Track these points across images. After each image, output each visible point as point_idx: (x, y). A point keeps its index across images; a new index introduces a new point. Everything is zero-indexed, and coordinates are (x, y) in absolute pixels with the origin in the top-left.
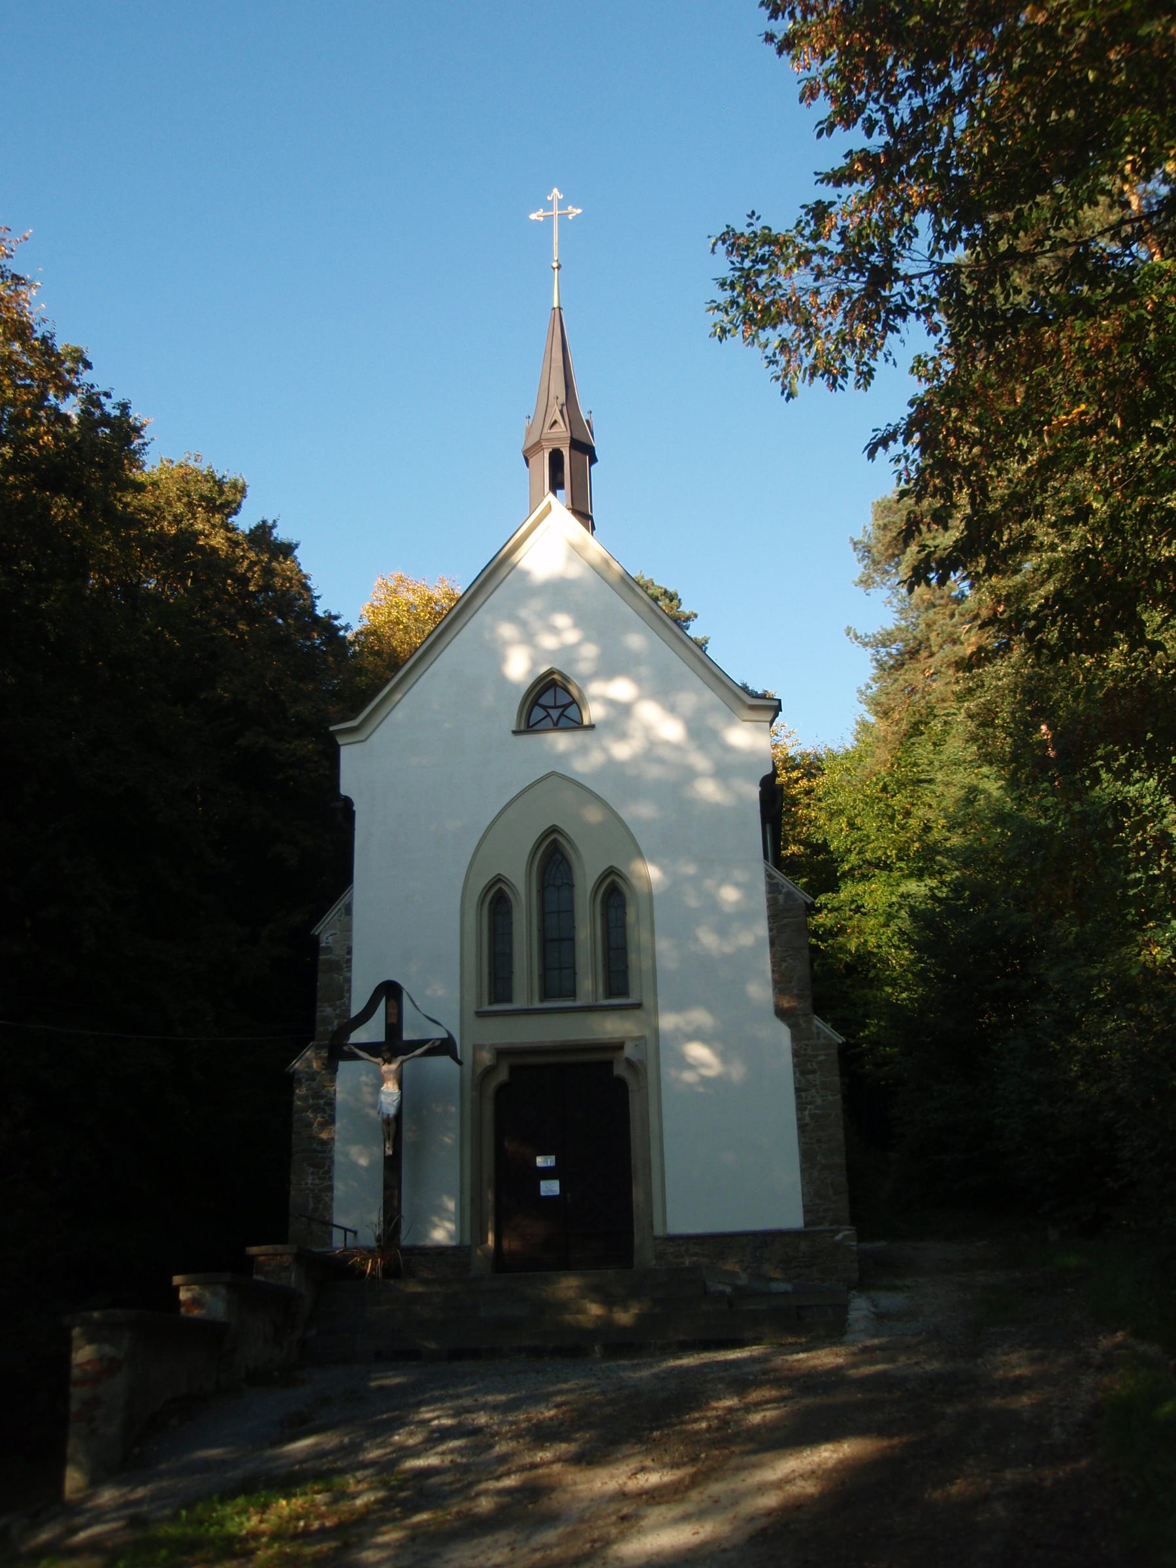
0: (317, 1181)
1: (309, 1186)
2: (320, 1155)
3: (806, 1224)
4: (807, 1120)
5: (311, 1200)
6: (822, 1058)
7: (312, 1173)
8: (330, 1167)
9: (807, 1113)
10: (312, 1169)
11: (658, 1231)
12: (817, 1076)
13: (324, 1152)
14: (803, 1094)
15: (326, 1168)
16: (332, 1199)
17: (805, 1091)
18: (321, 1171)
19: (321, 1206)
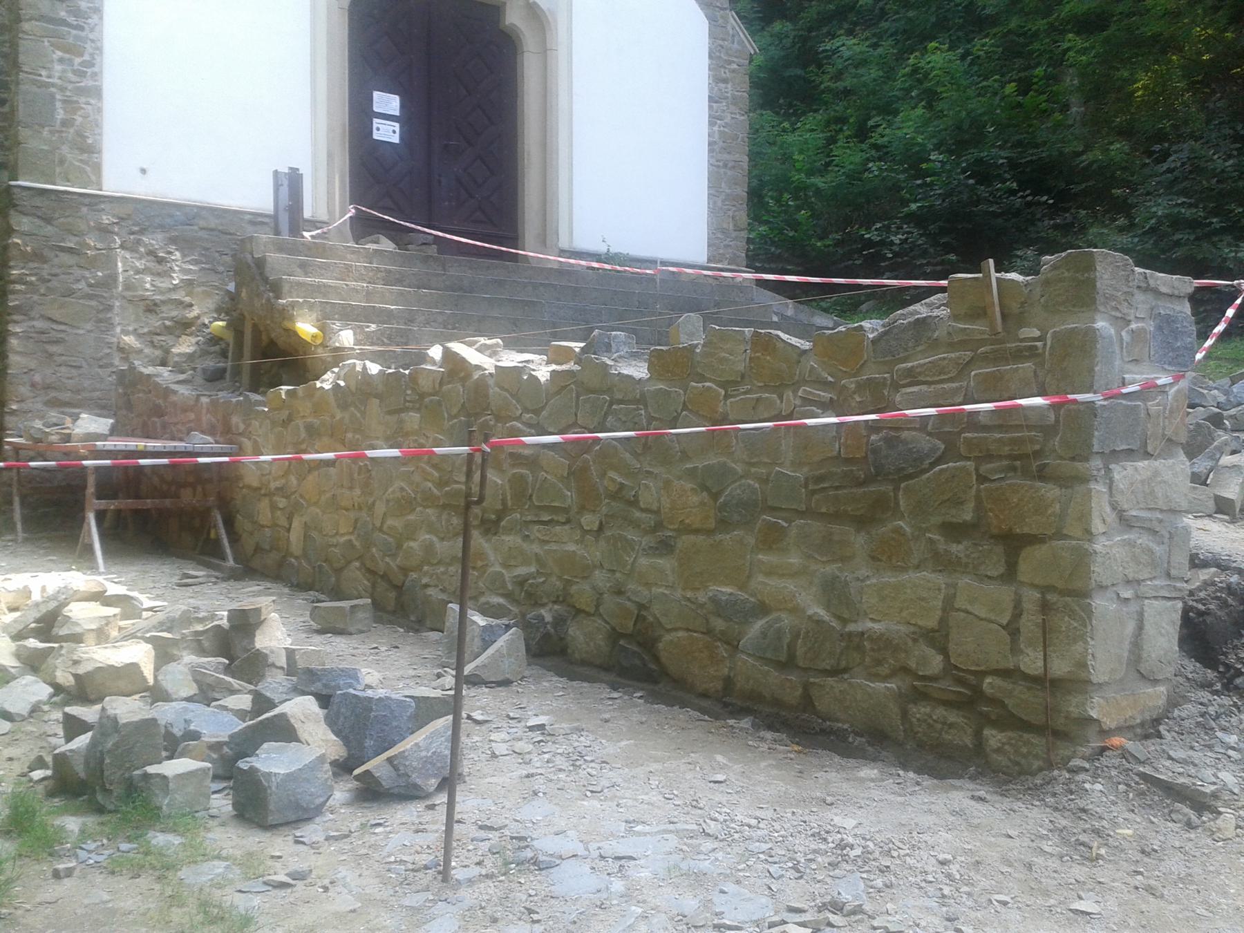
0: (70, 75)
1: (55, 81)
2: (74, 32)
3: (709, 261)
4: (717, 136)
5: (58, 105)
6: (735, 66)
7: (61, 60)
8: (92, 55)
9: (716, 128)
10: (59, 53)
11: (564, 243)
12: (729, 86)
13: (82, 28)
14: (714, 105)
15: (86, 57)
16: (100, 110)
17: (716, 102)
18: (77, 60)
19: (79, 120)
